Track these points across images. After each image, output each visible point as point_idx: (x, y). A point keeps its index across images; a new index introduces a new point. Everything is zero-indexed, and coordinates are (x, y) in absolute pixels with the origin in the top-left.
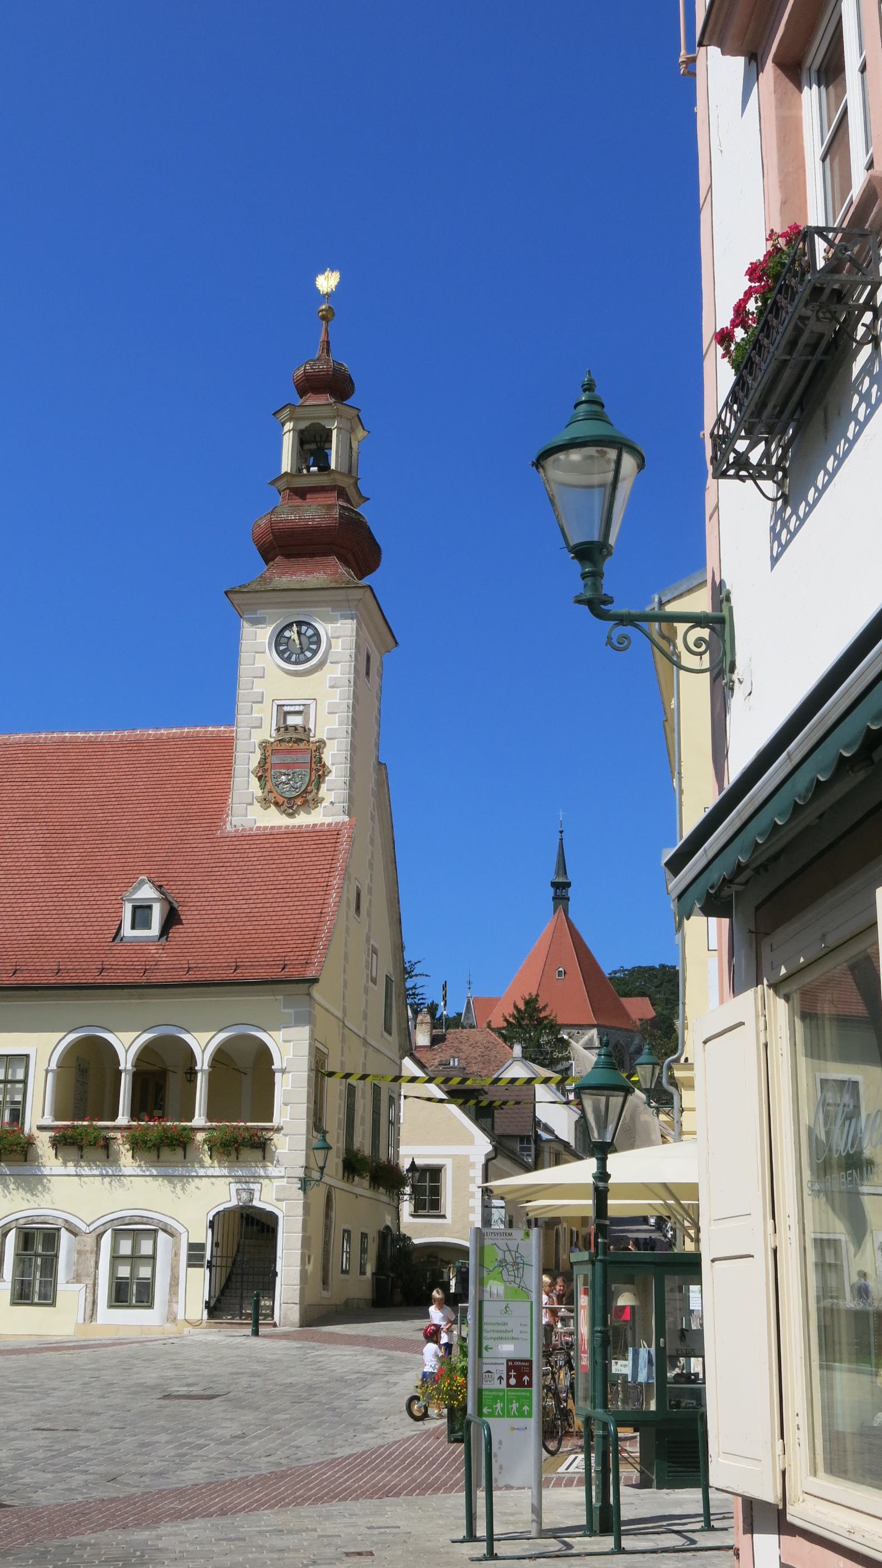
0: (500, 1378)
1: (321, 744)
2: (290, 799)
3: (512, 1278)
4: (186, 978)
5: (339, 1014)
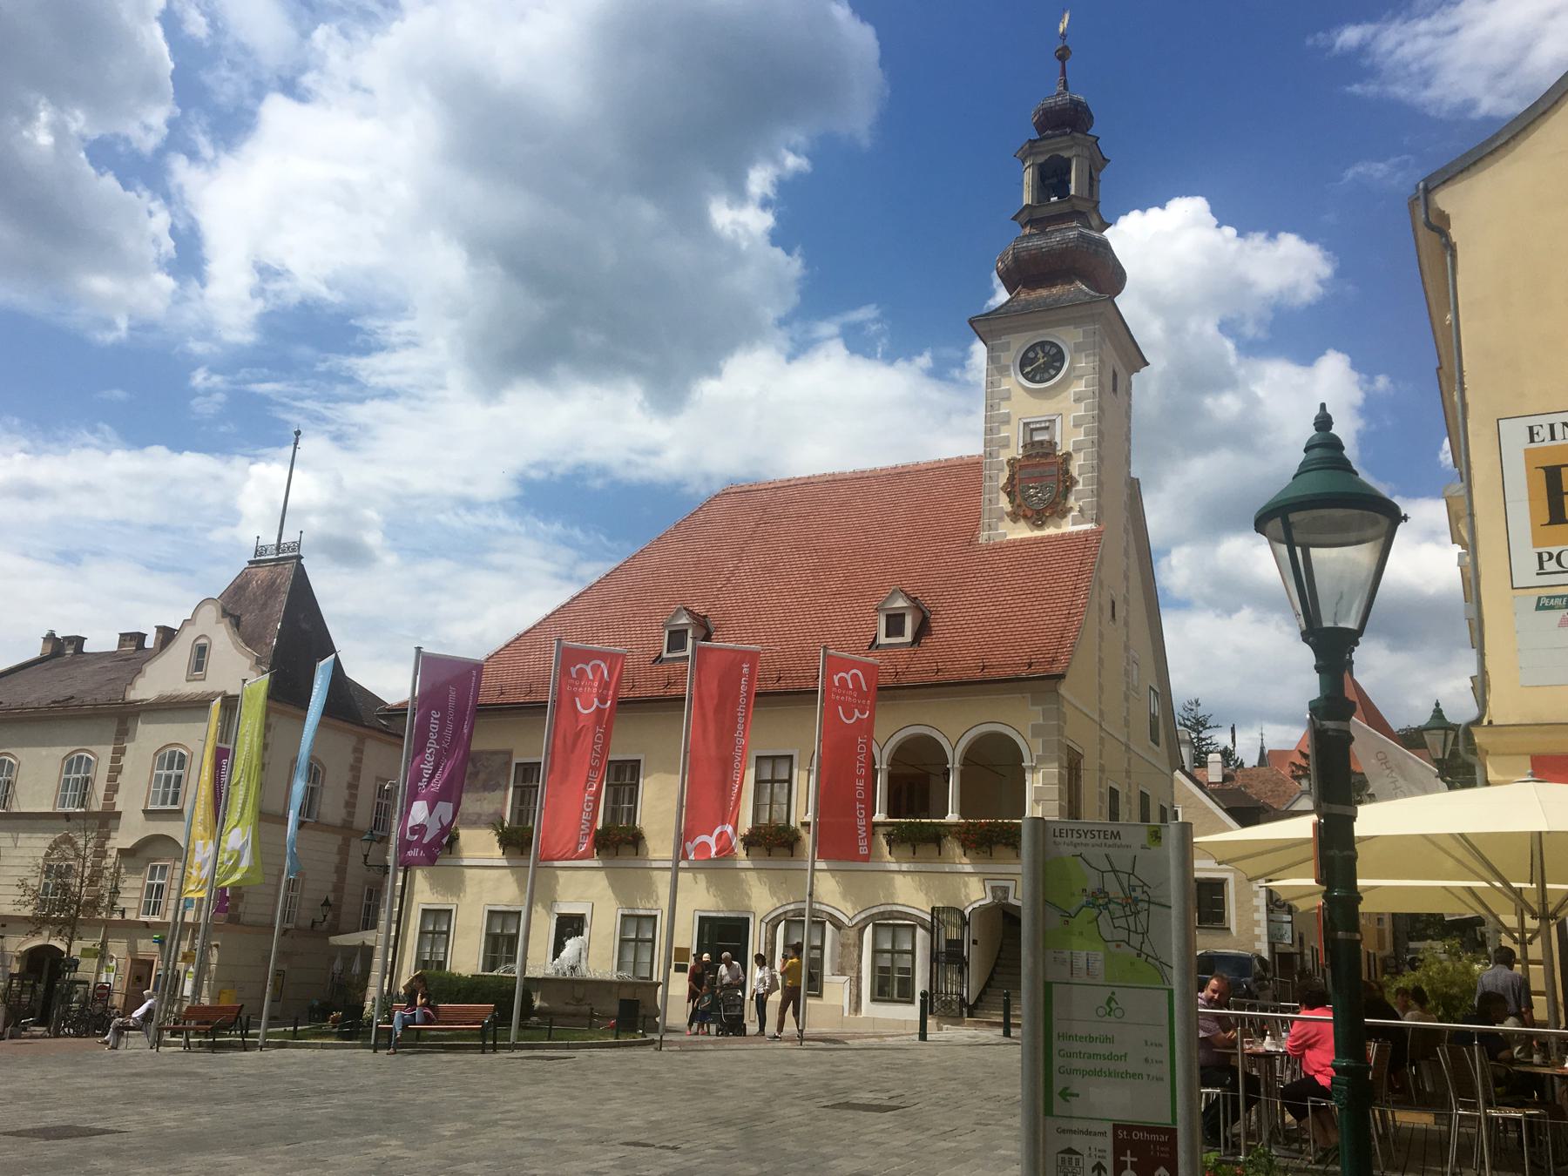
0: (1099, 1167)
1: (1068, 456)
2: (1038, 512)
3: (1123, 935)
4: (935, 679)
5: (1096, 717)
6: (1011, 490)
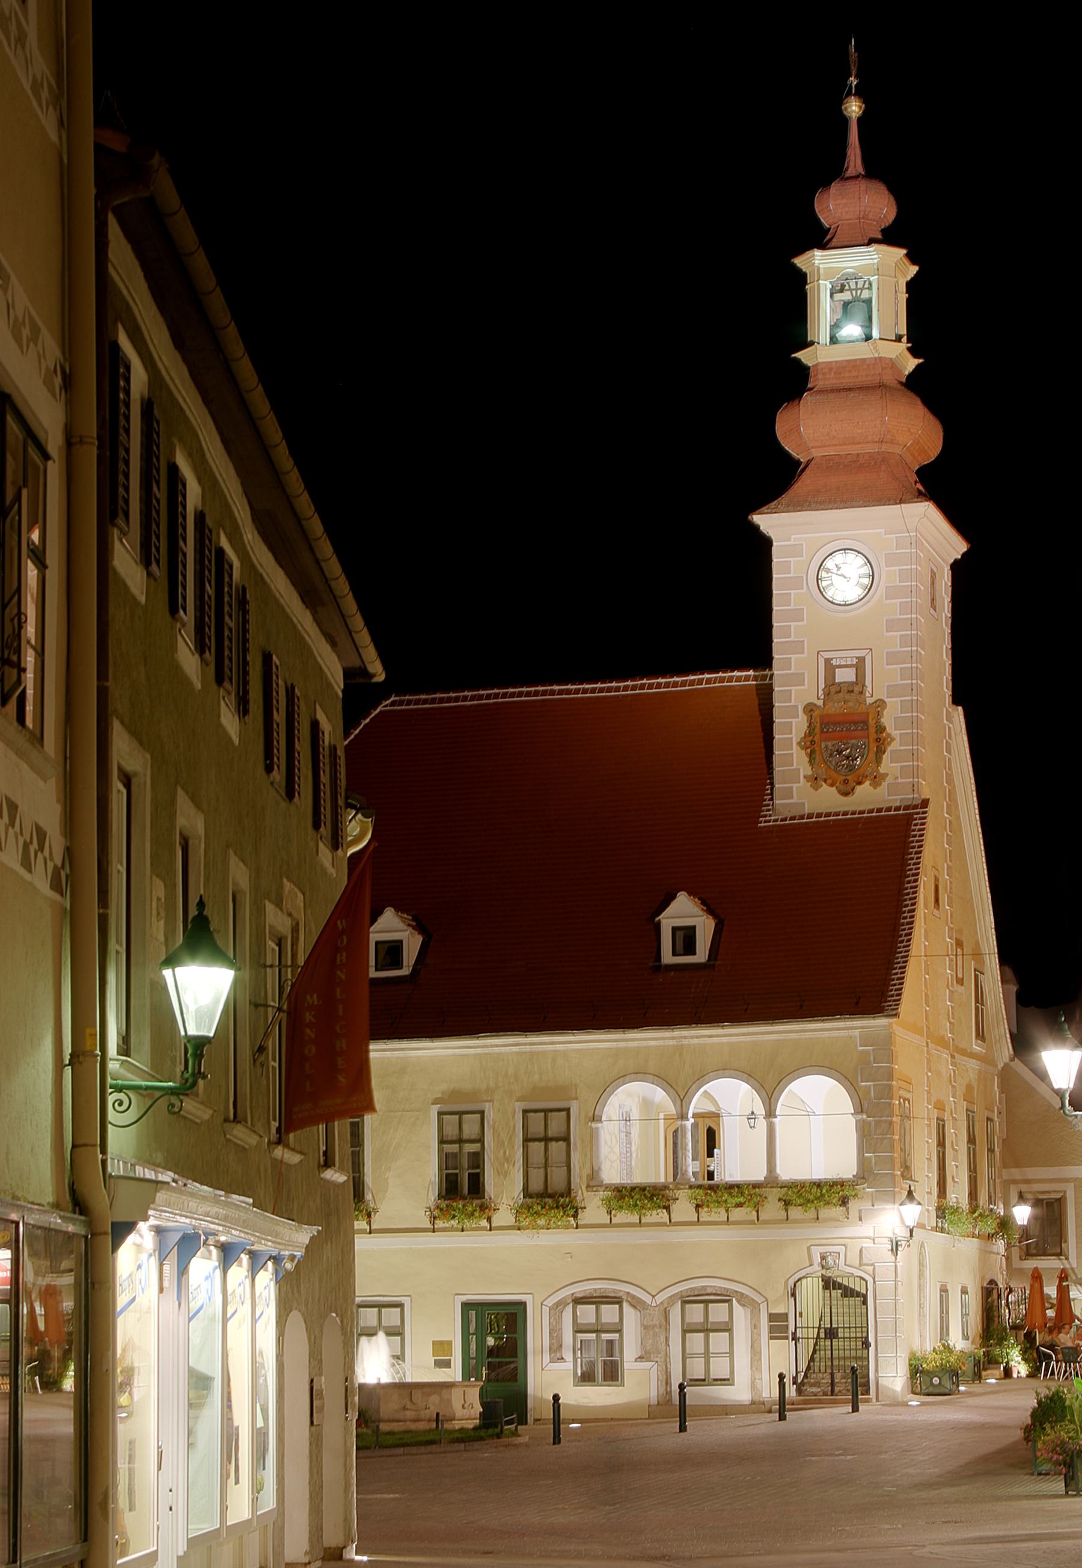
1: (881, 704)
6: (810, 744)
